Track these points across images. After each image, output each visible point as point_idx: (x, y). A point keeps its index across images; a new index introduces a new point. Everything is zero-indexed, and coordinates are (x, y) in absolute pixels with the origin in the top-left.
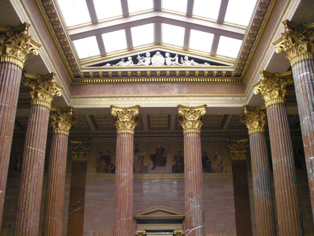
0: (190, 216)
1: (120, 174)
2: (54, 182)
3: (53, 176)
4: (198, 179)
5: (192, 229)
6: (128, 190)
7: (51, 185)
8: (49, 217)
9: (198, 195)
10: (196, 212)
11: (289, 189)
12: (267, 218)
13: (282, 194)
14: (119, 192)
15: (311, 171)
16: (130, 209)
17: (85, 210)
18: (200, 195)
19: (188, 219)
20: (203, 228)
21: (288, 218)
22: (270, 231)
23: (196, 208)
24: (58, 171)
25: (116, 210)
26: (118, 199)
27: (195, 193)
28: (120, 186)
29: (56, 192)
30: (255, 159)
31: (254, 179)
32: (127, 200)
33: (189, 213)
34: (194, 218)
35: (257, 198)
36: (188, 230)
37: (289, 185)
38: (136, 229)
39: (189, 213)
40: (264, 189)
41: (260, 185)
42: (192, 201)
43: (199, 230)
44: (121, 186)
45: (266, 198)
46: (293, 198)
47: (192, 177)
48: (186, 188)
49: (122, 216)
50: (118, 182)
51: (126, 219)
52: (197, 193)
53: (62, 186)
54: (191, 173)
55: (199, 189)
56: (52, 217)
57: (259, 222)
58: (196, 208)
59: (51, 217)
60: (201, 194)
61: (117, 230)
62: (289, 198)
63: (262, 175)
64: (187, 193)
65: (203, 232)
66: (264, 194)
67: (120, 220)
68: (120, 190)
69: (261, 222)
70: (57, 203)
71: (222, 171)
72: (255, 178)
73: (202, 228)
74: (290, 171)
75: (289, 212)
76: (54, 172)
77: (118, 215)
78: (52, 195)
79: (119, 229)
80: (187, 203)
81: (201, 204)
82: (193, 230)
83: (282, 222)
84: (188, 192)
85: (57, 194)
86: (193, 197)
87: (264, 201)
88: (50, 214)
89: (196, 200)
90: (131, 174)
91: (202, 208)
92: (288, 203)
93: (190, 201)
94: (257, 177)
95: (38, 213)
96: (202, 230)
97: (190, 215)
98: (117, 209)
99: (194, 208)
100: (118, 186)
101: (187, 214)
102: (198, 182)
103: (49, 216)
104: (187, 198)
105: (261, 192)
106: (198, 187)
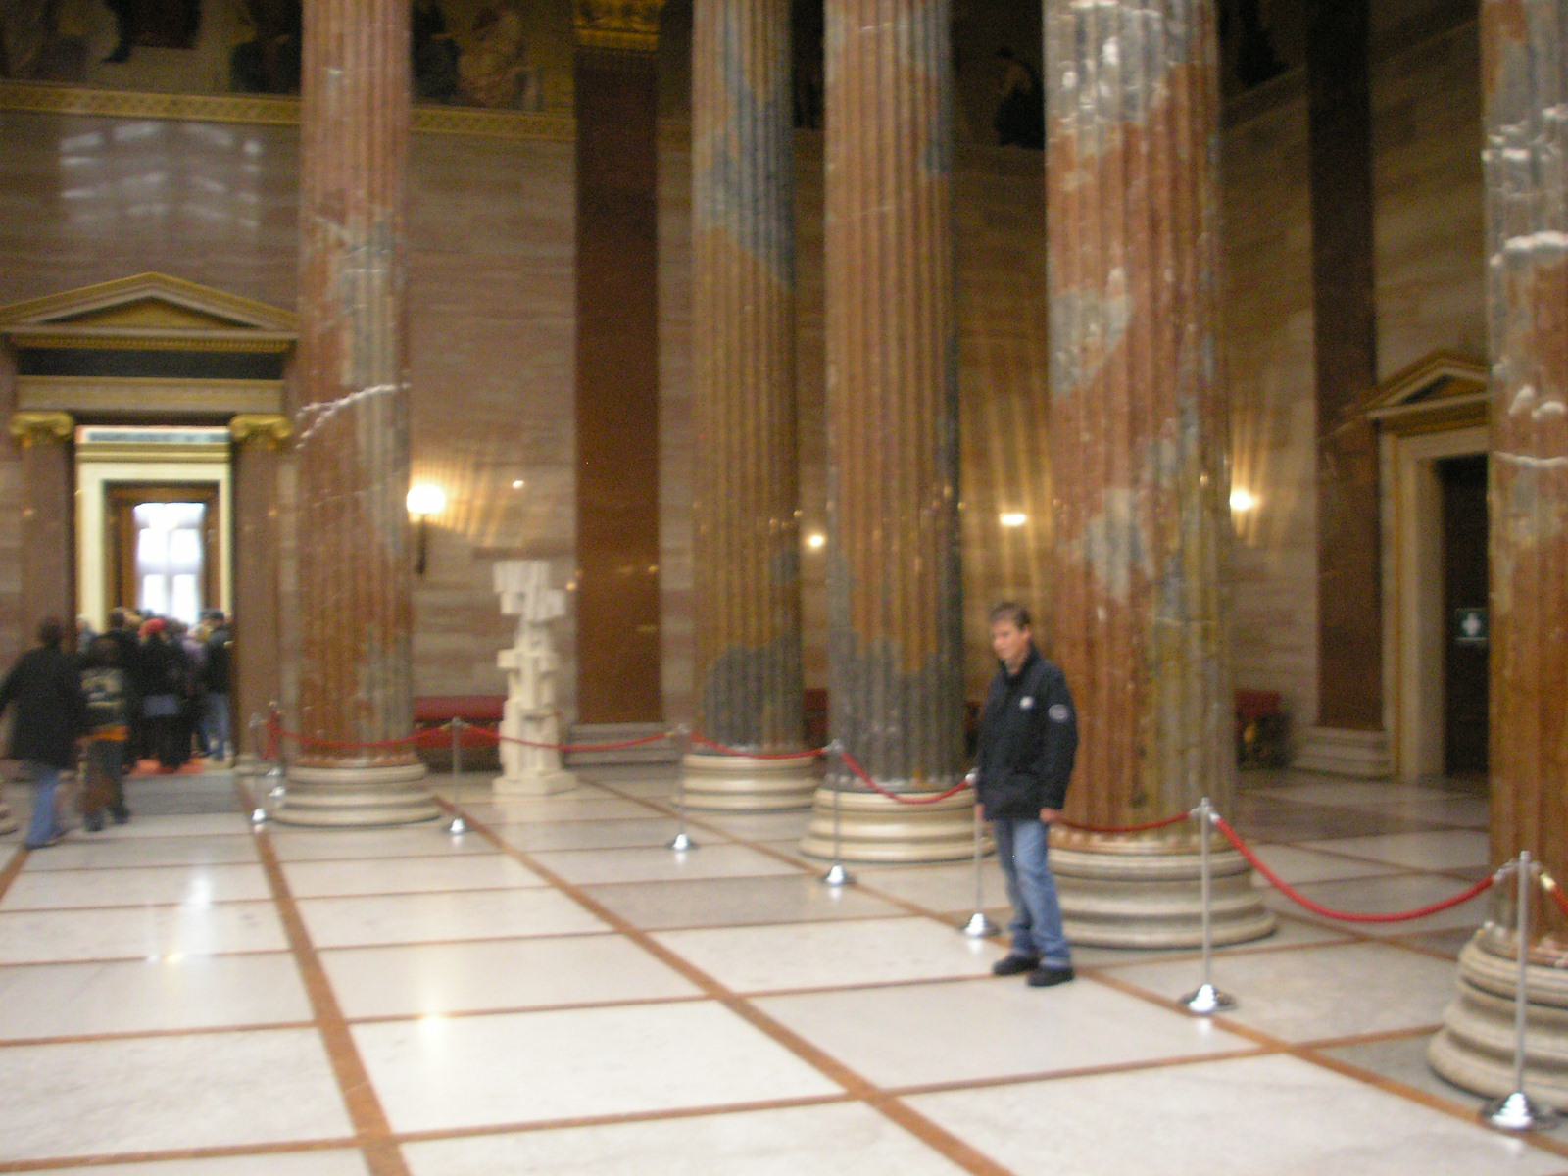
0: (330, 323)
5: (332, 400)
11: (907, 195)
13: (865, 220)
15: (1070, 79)
18: (390, 210)
20: (399, 401)
21: (885, 355)
27: (362, 193)
30: (720, 30)
31: (703, 148)
34: (347, 340)
37: (907, 177)
38: (13, 404)
39: (325, 308)
41: (734, 177)
42: (341, 244)
43: (378, 407)
45: (762, 250)
46: (924, 250)
52: (372, 195)
54: (340, 78)
58: (362, 284)
62: (900, 244)
63: (747, 122)
66: (748, 230)
74: (920, 95)
75: (893, 321)
83: (851, 379)
86: (351, 218)
89: (362, 237)
91: (400, 283)
92: (892, 273)
93: (332, 238)
94: (720, 131)
105: (734, 216)
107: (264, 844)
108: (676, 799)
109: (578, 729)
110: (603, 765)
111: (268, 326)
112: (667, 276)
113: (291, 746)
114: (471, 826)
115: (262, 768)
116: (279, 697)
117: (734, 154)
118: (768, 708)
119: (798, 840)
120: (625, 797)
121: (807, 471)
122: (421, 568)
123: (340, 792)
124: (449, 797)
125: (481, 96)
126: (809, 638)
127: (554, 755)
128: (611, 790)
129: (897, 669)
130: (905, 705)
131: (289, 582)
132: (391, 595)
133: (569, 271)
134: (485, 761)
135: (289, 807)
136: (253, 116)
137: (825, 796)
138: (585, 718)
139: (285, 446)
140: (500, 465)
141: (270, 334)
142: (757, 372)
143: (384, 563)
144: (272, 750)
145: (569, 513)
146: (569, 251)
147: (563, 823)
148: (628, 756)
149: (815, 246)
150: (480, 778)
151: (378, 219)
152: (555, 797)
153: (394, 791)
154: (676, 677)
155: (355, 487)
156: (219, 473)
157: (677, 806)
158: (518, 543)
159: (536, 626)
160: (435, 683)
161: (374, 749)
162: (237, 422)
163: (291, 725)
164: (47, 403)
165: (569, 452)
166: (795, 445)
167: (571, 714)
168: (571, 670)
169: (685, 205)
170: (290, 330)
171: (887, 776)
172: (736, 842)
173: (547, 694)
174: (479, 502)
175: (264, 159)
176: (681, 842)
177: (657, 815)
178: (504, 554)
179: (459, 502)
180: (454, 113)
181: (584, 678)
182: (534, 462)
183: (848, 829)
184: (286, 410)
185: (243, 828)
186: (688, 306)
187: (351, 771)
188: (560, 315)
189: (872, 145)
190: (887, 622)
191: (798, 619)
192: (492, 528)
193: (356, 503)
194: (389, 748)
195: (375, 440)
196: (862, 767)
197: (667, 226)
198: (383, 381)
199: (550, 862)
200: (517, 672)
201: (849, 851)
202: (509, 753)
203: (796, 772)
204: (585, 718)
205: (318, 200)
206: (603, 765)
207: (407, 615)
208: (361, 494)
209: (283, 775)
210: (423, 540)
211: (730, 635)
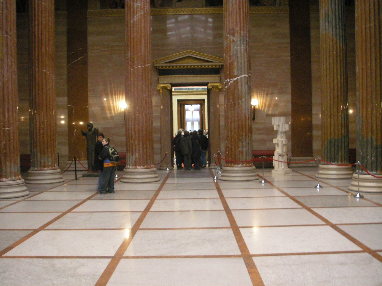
0: (231, 60)
1: (132, 3)
2: (38, 20)
3: (37, 11)
4: (243, 10)
5: (233, 79)
6: (143, 26)
7: (35, 24)
8: (35, 69)
9: (242, 32)
10: (239, 56)
11: (377, 21)
12: (337, 66)
14: (130, 29)
16: (146, 52)
17: (90, 61)
18: (245, 32)
19: (228, 65)
20: (249, 79)
21: (371, 63)
22: (339, 85)
23: (239, 50)
24: (43, 3)
25: (127, 55)
26: (130, 38)
27: (238, 29)
28: (132, 21)
29: (41, 34)
31: (322, 12)
32: (143, 40)
33: (230, 57)
34: (236, 64)
35: (324, 38)
36: (228, 80)
39: (230, 57)
40: (336, 25)
42: (233, 41)
43: (243, 80)
44: (134, 20)
45: (338, 38)
47: (234, 6)
48: (225, 22)
49: (136, 62)
50: (129, 15)
51: (141, 66)
52: (240, 29)
53: (50, 24)
55: (243, 23)
56: (40, 68)
57: (325, 72)
58: (239, 50)
59: (38, 68)
60: (246, 31)
61: (129, 82)
63: (333, 6)
64: (227, 29)
65: (249, 84)
66: (334, 33)
67: (133, 68)
68: (132, 26)
69: (328, 71)
70: (46, 49)
71: (274, 5)
72: (324, 10)
73: (247, 78)
75: (373, 55)
76: (36, 5)
77: (131, 61)
78: (37, 38)
79: (132, 80)
80: (226, 43)
81: (247, 45)
82: (234, 81)
84: (228, 27)
85: (43, 36)
86: (236, 34)
87: (335, 42)
88: (36, 64)
89: (239, 39)
90: (147, 2)
93: (231, 40)
94: (326, 8)
95: (13, 60)
96: (248, 81)
97: (230, 59)
98: (129, 53)
99: (237, 50)
100: (129, 21)
101: (227, 59)
102: (242, 14)
103: (35, 66)
104: (227, 37)
105: (330, 30)
106: (242, 21)
107: (217, 184)
108: (317, 176)
109: (291, 158)
110: (298, 167)
111: (216, 62)
112: (313, 46)
113: (223, 162)
114: (266, 181)
115: (216, 167)
116: (220, 150)
117: (330, 14)
118: (340, 154)
119: (348, 186)
120: (303, 175)
121: (350, 93)
122: (254, 119)
123: (235, 173)
124: (261, 174)
125: (265, 4)
126: (351, 136)
127: (287, 164)
128: (300, 173)
129: (375, 143)
130: (376, 153)
131: (222, 123)
132: (247, 126)
133: (289, 45)
134: (270, 166)
135: (222, 176)
136: (211, 12)
137: (355, 175)
138: (293, 155)
139: (220, 90)
140: (272, 94)
141: (217, 63)
142: (337, 69)
143: (246, 118)
144: (218, 163)
145: (290, 105)
146: (288, 40)
147: (288, 181)
148: (305, 165)
149: (353, 36)
150: (268, 170)
151: (242, 34)
152: (287, 175)
153: (248, 173)
154: (316, 145)
155: (238, 99)
156: (205, 97)
157: (318, 178)
158: (277, 113)
159: (281, 133)
160: (257, 147)
161: (243, 162)
162: (209, 85)
163: (223, 157)
164: (166, 82)
165: (289, 90)
166: (347, 87)
167: (290, 154)
168: (290, 143)
169: (318, 28)
170: (221, 62)
171: (372, 171)
172: (332, 186)
173: (285, 150)
174: (267, 103)
175: (214, 22)
176: (318, 187)
177: (311, 179)
178: (274, 115)
179: (262, 103)
180: (259, 8)
181: (293, 146)
182: (281, 92)
183: (361, 184)
184: (221, 81)
185: (212, 181)
186: (319, 53)
187: (237, 168)
188: (286, 56)
189: (367, 9)
190: (372, 131)
191: (348, 131)
192: (271, 109)
193: (239, 104)
194: (247, 162)
195: (243, 88)
196: (365, 168)
197: (313, 33)
198: (245, 74)
199: (285, 190)
200: (278, 144)
201: (361, 189)
202: (275, 164)
203: (347, 169)
204: (293, 155)
205: (228, 31)
206: (298, 167)
207: (251, 130)
208: (240, 101)
209: (221, 168)
210: (254, 111)
211: (331, 135)
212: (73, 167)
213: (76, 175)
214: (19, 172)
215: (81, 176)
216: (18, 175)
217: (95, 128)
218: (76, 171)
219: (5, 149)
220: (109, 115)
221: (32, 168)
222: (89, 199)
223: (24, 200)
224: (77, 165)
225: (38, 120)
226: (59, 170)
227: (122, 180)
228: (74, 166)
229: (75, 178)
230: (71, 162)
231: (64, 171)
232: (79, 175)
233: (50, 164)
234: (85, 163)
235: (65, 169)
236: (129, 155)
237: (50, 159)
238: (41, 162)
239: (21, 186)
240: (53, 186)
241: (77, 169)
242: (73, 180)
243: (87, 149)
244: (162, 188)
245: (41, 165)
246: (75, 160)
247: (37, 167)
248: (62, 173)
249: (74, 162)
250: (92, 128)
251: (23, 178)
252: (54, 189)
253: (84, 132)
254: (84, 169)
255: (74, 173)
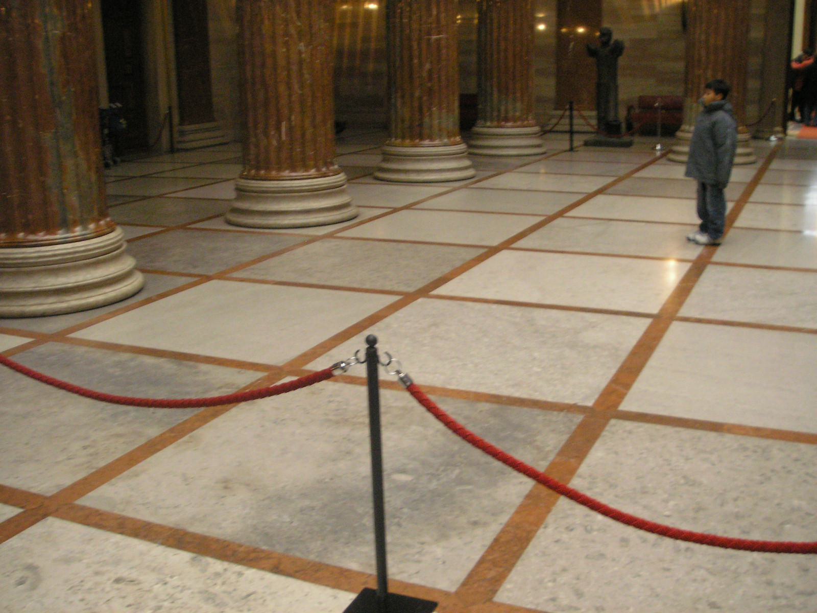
212: (564, 125)
213: (571, 141)
214: (457, 129)
215: (582, 143)
216: (455, 136)
217: (617, 42)
218: (571, 132)
219: (430, 78)
220: (646, 12)
221: (480, 122)
222: (600, 191)
223: (466, 187)
224: (575, 121)
225: (495, 21)
226: (536, 129)
227: (671, 156)
228: (567, 121)
229: (567, 147)
230: (560, 112)
231: (545, 132)
232: (578, 140)
233: (518, 114)
234: (590, 117)
235: (548, 128)
236: (689, 102)
237: (518, 105)
238: (499, 111)
239: (456, 158)
240: (522, 162)
241: (575, 128)
242: (565, 151)
243: (599, 85)
244: (759, 179)
245: (498, 116)
246: (571, 109)
247: (492, 121)
248: (541, 135)
249: (568, 113)
250: (609, 40)
251: (464, 142)
252: (522, 169)
253: (593, 47)
254: (589, 129)
255: (567, 136)
